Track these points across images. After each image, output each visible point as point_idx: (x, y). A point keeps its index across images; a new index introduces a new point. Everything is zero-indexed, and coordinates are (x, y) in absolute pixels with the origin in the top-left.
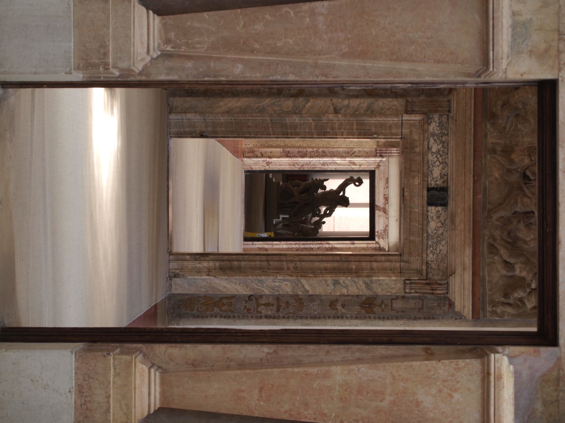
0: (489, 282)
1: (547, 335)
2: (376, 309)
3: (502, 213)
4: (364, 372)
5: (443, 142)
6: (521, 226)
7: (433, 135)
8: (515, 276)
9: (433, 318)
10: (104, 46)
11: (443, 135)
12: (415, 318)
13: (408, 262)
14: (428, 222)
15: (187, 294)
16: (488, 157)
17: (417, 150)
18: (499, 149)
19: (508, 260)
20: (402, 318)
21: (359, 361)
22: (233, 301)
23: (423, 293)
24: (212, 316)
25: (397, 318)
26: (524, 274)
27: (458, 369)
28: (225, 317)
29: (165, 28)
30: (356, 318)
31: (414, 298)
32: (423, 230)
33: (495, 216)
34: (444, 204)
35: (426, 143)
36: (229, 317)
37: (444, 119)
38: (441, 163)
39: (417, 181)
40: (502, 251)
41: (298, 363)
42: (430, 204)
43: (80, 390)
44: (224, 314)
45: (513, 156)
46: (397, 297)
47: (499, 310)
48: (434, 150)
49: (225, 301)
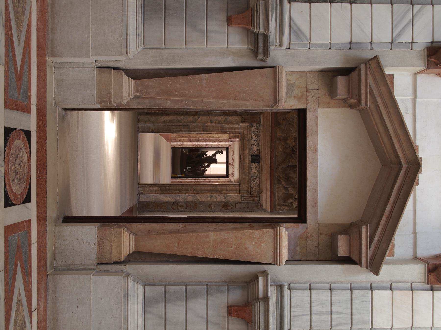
0: (278, 196)
1: (302, 218)
2: (229, 208)
3: (283, 166)
4: (223, 235)
6: (291, 171)
7: (253, 132)
10: (109, 93)
11: (258, 132)
12: (246, 212)
13: (242, 187)
17: (247, 139)
20: (240, 212)
21: (221, 230)
23: (249, 201)
24: (157, 211)
25: (238, 212)
26: (292, 192)
28: (163, 211)
29: (136, 85)
30: (220, 212)
31: (245, 203)
33: (280, 167)
34: (258, 162)
35: (250, 136)
36: (165, 212)
37: (258, 125)
38: (257, 144)
39: (246, 152)
40: (283, 182)
41: (195, 231)
42: (252, 162)
43: (99, 244)
45: (288, 141)
46: (238, 203)
48: (254, 139)
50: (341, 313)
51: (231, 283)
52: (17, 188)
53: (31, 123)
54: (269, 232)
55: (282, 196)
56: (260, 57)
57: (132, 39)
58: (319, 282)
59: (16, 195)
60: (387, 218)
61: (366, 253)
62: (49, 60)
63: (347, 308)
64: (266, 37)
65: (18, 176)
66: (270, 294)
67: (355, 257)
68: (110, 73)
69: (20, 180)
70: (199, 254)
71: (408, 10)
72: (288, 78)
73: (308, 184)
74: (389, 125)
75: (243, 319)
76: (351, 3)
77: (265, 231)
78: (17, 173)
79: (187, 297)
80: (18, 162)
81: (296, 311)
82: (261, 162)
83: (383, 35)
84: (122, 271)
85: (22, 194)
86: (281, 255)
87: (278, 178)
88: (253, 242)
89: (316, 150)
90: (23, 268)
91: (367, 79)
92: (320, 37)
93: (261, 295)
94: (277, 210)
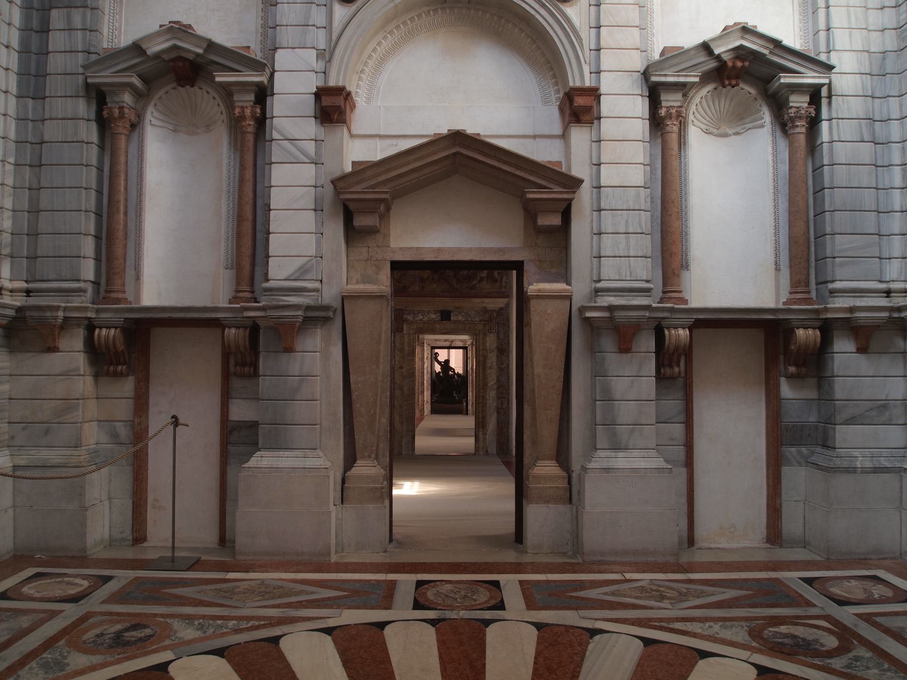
1: (518, 266)
21: (531, 359)
29: (363, 458)
41: (533, 390)
42: (450, 320)
43: (547, 502)
50: (627, 222)
51: (592, 349)
52: (483, 596)
53: (407, 580)
54: (533, 304)
56: (331, 314)
57: (310, 463)
58: (592, 247)
59: (491, 598)
60: (517, 169)
61: (557, 193)
62: (334, 558)
63: (622, 215)
64: (308, 308)
65: (469, 595)
66: (606, 304)
67: (564, 206)
68: (349, 488)
69: (474, 593)
70: (560, 385)
71: (278, 144)
72: (355, 281)
73: (478, 259)
74: (411, 167)
75: (634, 334)
76: (270, 210)
77: (532, 309)
78: (465, 596)
79: (609, 399)
80: (452, 595)
82: (450, 309)
83: (308, 173)
84: (579, 475)
85: (489, 591)
88: (546, 322)
89: (439, 250)
90: (575, 590)
91: (356, 192)
92: (308, 245)
93: (606, 314)
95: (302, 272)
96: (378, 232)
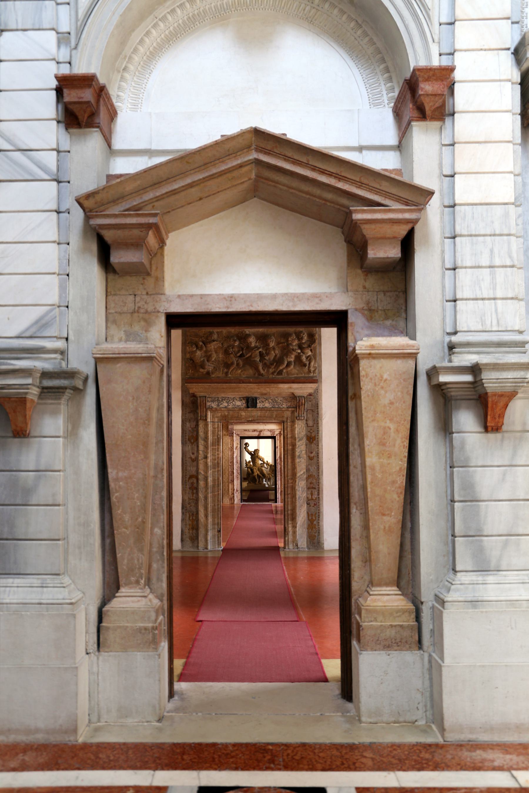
2: (313, 435)
3: (260, 368)
4: (370, 441)
5: (222, 400)
6: (267, 358)
7: (218, 405)
8: (294, 361)
9: (318, 404)
11: (218, 400)
12: (318, 414)
13: (287, 418)
14: (266, 407)
15: (307, 539)
16: (230, 376)
17: (226, 413)
18: (226, 370)
19: (285, 365)
20: (318, 421)
22: (310, 513)
24: (319, 525)
25: (318, 424)
26: (293, 356)
27: (367, 375)
28: (319, 518)
30: (318, 446)
31: (307, 415)
32: (269, 410)
33: (262, 371)
34: (256, 399)
35: (223, 409)
36: (319, 515)
37: (209, 399)
38: (233, 401)
39: (243, 414)
40: (281, 368)
41: (364, 487)
42: (256, 407)
44: (317, 518)
45: (229, 363)
46: (307, 424)
47: (312, 369)
48: (226, 405)
49: (310, 518)
55: (298, 368)
57: (51, 595)
64: (45, 375)
67: (403, 231)
70: (401, 480)
77: (362, 373)
81: (491, 323)
82: (256, 395)
86: (403, 347)
87: (275, 374)
89: (231, 298)
93: (468, 378)
94: (315, 375)
95: (40, 326)
96: (148, 274)
